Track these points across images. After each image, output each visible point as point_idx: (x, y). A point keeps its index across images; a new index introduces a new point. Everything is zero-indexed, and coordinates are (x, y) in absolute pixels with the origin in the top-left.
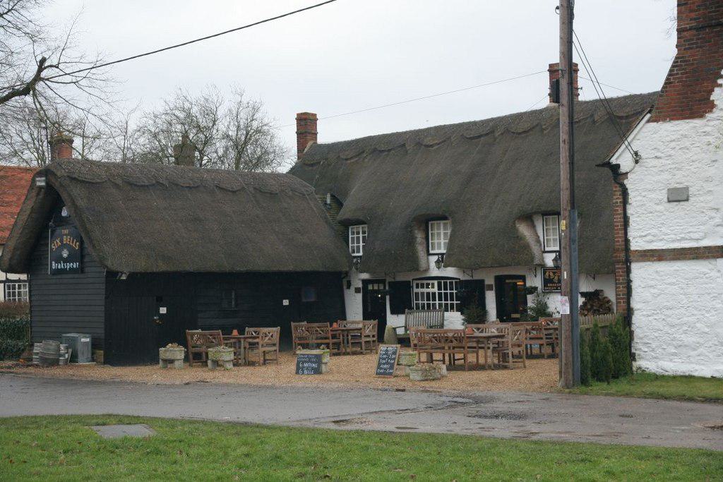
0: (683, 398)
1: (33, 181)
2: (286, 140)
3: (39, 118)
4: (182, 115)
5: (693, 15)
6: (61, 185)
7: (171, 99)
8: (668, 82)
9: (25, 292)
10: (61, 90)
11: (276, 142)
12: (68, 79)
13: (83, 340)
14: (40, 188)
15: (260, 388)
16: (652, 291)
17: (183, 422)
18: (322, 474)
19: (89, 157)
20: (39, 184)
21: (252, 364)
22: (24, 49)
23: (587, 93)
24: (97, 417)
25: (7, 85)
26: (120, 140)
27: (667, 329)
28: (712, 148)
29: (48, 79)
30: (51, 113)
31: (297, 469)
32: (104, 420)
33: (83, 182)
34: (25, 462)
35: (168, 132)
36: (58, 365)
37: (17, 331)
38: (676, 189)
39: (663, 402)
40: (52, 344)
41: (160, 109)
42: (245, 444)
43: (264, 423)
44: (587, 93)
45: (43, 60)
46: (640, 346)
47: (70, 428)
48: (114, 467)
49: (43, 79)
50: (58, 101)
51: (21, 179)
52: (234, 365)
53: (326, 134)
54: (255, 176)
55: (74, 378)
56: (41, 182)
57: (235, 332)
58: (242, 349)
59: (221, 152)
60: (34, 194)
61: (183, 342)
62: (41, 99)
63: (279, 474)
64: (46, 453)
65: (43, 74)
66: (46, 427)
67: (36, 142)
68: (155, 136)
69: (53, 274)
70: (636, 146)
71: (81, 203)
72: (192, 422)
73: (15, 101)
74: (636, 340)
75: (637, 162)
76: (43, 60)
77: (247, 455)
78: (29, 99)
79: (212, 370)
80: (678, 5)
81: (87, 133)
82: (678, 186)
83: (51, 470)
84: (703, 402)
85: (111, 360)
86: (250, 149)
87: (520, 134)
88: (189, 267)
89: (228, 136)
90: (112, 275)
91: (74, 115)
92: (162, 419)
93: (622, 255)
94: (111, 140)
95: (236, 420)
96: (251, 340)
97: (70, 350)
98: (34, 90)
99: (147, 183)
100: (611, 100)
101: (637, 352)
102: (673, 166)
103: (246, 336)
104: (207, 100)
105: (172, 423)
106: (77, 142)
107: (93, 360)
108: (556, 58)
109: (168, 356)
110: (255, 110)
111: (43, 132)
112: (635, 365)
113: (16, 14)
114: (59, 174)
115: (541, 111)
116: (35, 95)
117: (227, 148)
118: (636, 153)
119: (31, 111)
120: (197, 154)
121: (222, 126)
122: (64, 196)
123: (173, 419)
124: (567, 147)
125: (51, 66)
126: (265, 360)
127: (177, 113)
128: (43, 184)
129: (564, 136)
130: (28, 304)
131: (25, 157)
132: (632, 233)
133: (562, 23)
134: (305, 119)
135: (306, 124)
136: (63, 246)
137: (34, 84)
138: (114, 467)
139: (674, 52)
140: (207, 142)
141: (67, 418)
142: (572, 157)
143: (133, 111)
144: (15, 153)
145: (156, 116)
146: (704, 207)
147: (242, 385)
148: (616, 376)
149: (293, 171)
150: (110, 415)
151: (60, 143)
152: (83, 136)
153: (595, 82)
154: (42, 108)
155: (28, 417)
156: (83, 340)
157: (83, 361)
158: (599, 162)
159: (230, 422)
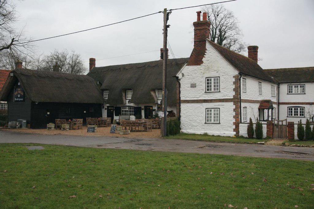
0: (193, 140)
1: (10, 74)
2: (86, 65)
3: (12, 56)
4: (56, 57)
5: (198, 38)
6: (18, 76)
7: (53, 52)
8: (191, 55)
9: (6, 107)
10: (19, 48)
11: (83, 66)
12: (21, 45)
13: (24, 121)
14: (12, 76)
15: (77, 136)
16: (186, 111)
17: (53, 145)
18: (93, 160)
19: (27, 68)
20: (11, 75)
21: (75, 129)
22: (8, 35)
23: (170, 57)
24: (27, 144)
25: (2, 46)
26: (37, 63)
27: (189, 121)
28: (202, 73)
29: (15, 45)
30: (16, 54)
31: (86, 159)
32: (29, 145)
33: (25, 75)
34: (4, 156)
35: (52, 62)
36: (16, 128)
37: (4, 118)
38: (193, 84)
39: (187, 141)
40: (14, 122)
41: (49, 55)
42: (71, 152)
43: (77, 146)
44: (170, 57)
45: (13, 39)
46: (182, 126)
47: (19, 147)
48: (32, 158)
49: (13, 45)
50: (18, 51)
51: (6, 73)
52: (69, 129)
53: (98, 65)
54: (77, 76)
55: (21, 132)
56: (12, 75)
57: (70, 120)
58: (72, 125)
59: (67, 68)
60: (10, 78)
61: (54, 122)
62: (12, 50)
63: (81, 160)
64: (11, 154)
65: (13, 43)
66: (11, 146)
67: (11, 63)
68: (48, 62)
69: (15, 102)
70: (183, 72)
71: (24, 81)
72: (56, 145)
73: (4, 50)
74: (181, 124)
75: (183, 76)
76: (13, 39)
77: (72, 155)
78: (9, 50)
79: (63, 131)
80: (195, 35)
81: (27, 61)
82: (193, 83)
83: (12, 159)
84: (197, 141)
85: (33, 127)
86: (75, 68)
87: (152, 67)
88: (56, 101)
89: (69, 64)
90: (33, 103)
91: (23, 55)
92: (47, 145)
93: (178, 101)
94: (34, 63)
95: (69, 145)
96: (74, 122)
97: (20, 124)
98: (10, 47)
99: (44, 76)
100: (177, 59)
101: (181, 127)
102: (193, 78)
103: (73, 121)
104: (63, 53)
105: (50, 146)
106: (24, 64)
107: (27, 127)
108: (162, 47)
109: (50, 126)
110: (78, 57)
111: (13, 60)
112: (181, 131)
113: (5, 25)
114: (18, 72)
115: (158, 61)
116: (10, 49)
117: (69, 67)
118: (183, 74)
119: (9, 53)
120: (60, 68)
121: (68, 61)
122: (19, 79)
123: (50, 145)
124: (165, 71)
125: (16, 41)
126: (78, 128)
127: (54, 56)
128: (13, 75)
129: (164, 68)
130: (7, 110)
131: (7, 67)
132: (181, 95)
133: (164, 37)
134: (92, 60)
135: (92, 61)
136: (18, 94)
137: (10, 45)
138: (32, 158)
139: (193, 47)
140: (63, 65)
141: (18, 144)
142: (166, 74)
143: (41, 55)
144: (4, 66)
145: (48, 57)
146: (200, 89)
147: (71, 135)
148: (176, 134)
149: (88, 74)
150: (31, 143)
151: (18, 63)
152: (26, 62)
153: (173, 54)
154: (13, 53)
155: (6, 143)
156: (24, 121)
157: (24, 127)
158: (173, 76)
159: (67, 146)
